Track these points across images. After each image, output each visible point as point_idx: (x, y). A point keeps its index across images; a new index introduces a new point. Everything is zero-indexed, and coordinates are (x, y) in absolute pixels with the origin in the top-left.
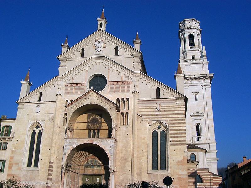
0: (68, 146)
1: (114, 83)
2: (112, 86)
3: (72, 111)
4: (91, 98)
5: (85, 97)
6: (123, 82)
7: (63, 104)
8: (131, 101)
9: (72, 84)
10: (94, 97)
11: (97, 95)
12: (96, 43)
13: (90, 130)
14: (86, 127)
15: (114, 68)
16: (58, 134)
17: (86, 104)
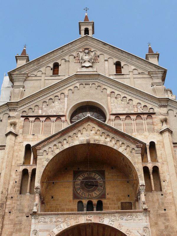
0: (41, 231)
1: (121, 117)
2: (118, 121)
3: (47, 157)
4: (88, 132)
5: (75, 131)
6: (138, 115)
7: (20, 153)
8: (157, 147)
9: (37, 117)
10: (93, 132)
11: (100, 129)
12: (81, 54)
13: (80, 203)
14: (72, 194)
15: (117, 92)
16: (7, 211)
17: (76, 143)
